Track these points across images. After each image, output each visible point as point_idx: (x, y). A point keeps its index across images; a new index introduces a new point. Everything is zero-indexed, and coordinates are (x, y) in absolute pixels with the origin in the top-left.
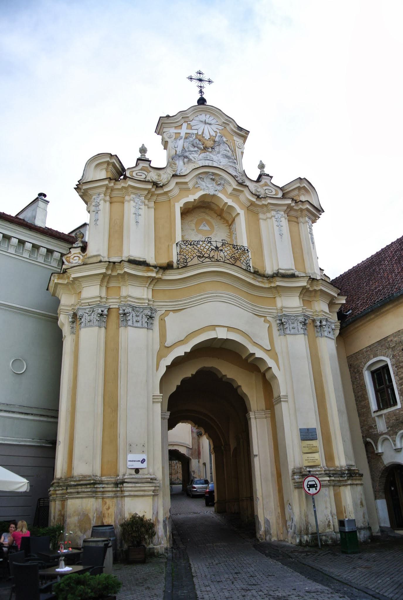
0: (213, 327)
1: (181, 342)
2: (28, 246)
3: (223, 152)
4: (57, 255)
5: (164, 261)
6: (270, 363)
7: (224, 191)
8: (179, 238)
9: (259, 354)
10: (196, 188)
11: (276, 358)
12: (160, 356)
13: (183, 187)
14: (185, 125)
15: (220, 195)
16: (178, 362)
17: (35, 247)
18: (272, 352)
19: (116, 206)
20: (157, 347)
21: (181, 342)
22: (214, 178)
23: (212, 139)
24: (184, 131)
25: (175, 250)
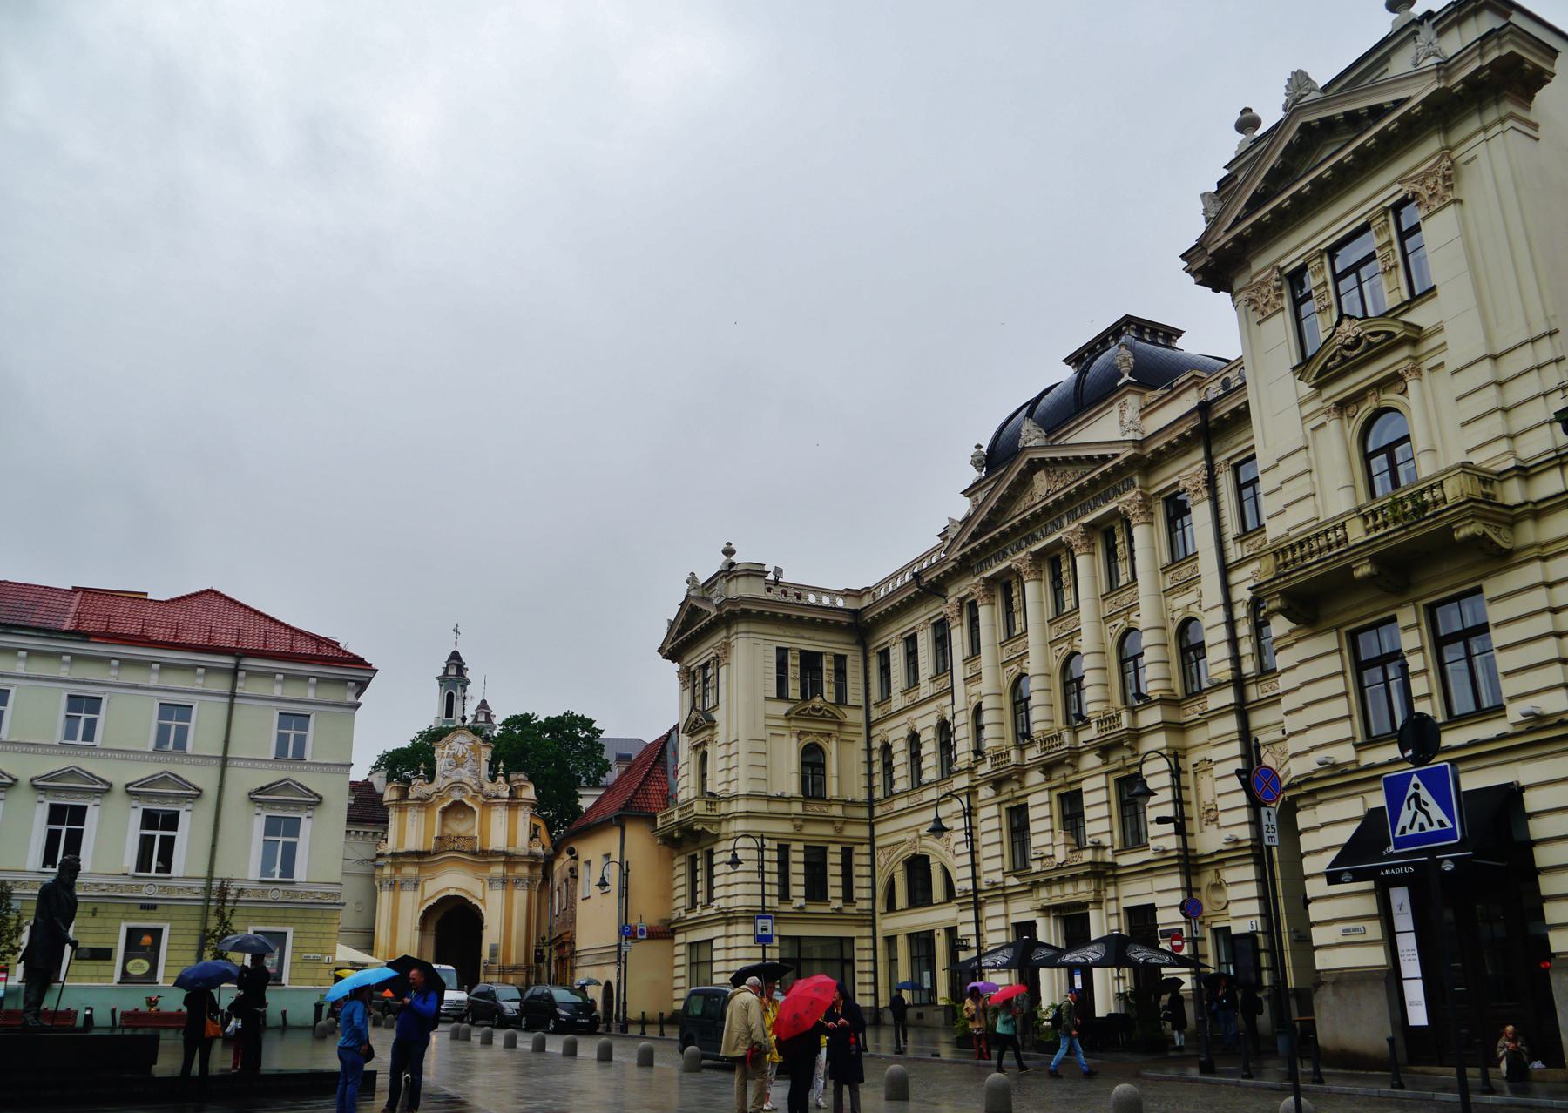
0: (448, 889)
1: (431, 897)
2: (361, 833)
3: (469, 767)
4: (380, 834)
5: (427, 849)
6: (481, 907)
7: (466, 797)
8: (436, 835)
9: (475, 902)
10: (450, 797)
11: (485, 905)
12: (421, 905)
13: (442, 798)
14: (447, 746)
15: (464, 800)
16: (430, 907)
17: (366, 833)
18: (482, 900)
19: (403, 814)
20: (419, 899)
21: (431, 897)
22: (461, 789)
23: (463, 755)
24: (446, 751)
25: (433, 841)
